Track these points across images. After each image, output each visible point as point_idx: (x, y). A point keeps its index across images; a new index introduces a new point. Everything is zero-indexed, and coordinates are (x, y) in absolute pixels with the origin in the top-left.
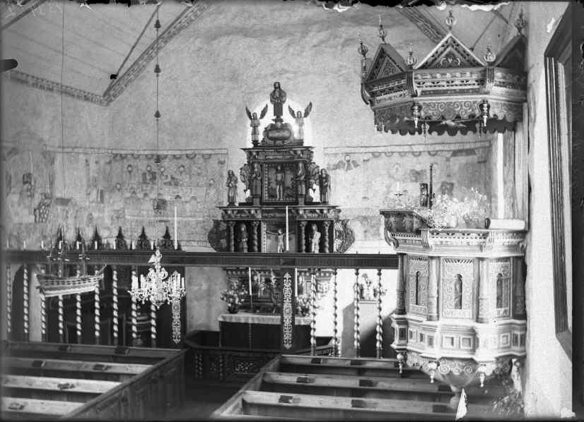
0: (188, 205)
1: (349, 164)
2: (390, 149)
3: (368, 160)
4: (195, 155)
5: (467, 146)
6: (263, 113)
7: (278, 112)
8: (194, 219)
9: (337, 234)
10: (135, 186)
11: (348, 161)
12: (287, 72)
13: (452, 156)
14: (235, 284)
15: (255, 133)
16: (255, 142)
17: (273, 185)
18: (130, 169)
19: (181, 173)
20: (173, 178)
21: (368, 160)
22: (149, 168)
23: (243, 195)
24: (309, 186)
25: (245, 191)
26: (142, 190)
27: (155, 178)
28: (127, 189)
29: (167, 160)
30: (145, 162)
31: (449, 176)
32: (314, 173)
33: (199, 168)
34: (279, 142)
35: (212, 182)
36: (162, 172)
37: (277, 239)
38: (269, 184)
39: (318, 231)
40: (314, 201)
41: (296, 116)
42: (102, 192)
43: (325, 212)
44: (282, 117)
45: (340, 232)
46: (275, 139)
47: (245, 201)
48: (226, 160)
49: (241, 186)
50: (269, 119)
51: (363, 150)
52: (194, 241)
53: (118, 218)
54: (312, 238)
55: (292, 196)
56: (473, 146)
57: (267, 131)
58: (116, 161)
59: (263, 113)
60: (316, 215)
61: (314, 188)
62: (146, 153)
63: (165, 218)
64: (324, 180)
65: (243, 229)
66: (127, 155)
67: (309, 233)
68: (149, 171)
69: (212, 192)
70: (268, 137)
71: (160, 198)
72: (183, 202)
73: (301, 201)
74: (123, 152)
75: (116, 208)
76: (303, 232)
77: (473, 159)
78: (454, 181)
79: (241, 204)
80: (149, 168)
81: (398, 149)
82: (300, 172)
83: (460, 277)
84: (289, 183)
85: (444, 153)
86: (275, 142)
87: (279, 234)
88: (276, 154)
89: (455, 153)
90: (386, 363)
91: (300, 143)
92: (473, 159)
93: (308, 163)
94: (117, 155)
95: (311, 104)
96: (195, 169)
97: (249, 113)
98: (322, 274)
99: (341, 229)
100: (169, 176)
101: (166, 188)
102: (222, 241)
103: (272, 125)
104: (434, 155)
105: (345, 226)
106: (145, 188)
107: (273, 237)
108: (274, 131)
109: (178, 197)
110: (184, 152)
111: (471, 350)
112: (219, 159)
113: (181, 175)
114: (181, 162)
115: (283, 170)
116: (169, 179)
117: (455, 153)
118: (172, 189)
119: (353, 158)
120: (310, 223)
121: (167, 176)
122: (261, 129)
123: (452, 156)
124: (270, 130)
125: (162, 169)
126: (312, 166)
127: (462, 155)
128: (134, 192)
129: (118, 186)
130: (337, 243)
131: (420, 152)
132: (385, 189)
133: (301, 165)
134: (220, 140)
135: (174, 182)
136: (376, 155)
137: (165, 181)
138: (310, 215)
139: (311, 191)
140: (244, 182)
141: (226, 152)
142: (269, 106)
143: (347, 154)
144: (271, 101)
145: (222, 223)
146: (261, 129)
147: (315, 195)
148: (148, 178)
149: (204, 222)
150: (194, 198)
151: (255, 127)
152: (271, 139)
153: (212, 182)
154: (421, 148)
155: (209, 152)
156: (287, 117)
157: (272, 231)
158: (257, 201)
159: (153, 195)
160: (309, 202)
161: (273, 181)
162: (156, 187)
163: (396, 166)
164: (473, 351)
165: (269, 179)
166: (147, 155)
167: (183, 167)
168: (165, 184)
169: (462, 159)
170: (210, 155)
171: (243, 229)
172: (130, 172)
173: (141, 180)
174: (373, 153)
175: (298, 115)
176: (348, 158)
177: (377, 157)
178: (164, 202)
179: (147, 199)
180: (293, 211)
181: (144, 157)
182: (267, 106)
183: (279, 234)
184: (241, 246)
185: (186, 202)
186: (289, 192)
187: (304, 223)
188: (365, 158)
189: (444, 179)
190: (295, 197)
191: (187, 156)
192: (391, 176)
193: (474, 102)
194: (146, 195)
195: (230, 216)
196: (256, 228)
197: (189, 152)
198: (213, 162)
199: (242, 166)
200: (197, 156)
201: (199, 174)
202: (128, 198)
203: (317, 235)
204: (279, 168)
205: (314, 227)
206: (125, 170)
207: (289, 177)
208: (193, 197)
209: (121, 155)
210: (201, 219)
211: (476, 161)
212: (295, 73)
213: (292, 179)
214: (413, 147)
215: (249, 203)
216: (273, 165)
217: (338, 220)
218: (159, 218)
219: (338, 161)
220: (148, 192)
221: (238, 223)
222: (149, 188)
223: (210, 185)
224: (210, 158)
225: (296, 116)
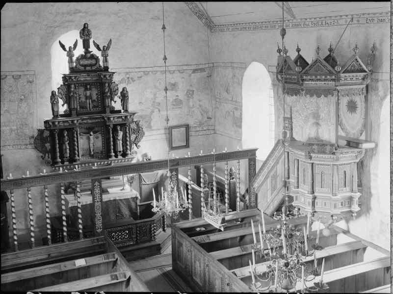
1: (130, 80)
2: (155, 69)
3: (141, 77)
4: (6, 76)
5: (201, 67)
6: (75, 45)
7: (86, 45)
11: (128, 78)
12: (80, 12)
13: (192, 73)
15: (71, 61)
16: (72, 70)
21: (141, 77)
23: (62, 109)
24: (112, 99)
25: (63, 105)
31: (191, 86)
34: (88, 68)
35: (23, 97)
37: (89, 139)
38: (79, 99)
39: (121, 130)
40: (115, 109)
41: (102, 49)
43: (129, 117)
44: (90, 50)
46: (85, 66)
47: (64, 113)
48: (34, 80)
49: (61, 102)
50: (79, 51)
51: (136, 70)
54: (118, 136)
55: (97, 107)
56: (203, 66)
57: (78, 59)
59: (75, 45)
60: (121, 120)
61: (115, 100)
65: (65, 135)
67: (115, 131)
69: (24, 105)
70: (80, 65)
73: (108, 110)
76: (111, 132)
77: (205, 74)
78: (194, 89)
79: (62, 116)
81: (158, 69)
83: (345, 172)
84: (95, 97)
85: (188, 71)
86: (85, 68)
87: (91, 135)
88: (86, 77)
89: (195, 71)
90: (231, 216)
91: (106, 69)
92: (205, 74)
93: (110, 82)
95: (111, 40)
97: (63, 46)
98: (126, 160)
103: (82, 55)
104: (182, 73)
105: (138, 125)
107: (85, 137)
108: (84, 60)
111: (348, 207)
112: (27, 78)
115: (90, 89)
117: (195, 71)
119: (131, 75)
120: (115, 126)
122: (74, 59)
123: (192, 73)
124: (80, 59)
126: (113, 85)
127: (198, 73)
130: (133, 137)
131: (174, 71)
132: (152, 96)
133: (107, 85)
134: (28, 63)
136: (146, 73)
138: (116, 120)
139: (112, 102)
140: (61, 98)
141: (33, 73)
142: (78, 42)
143: (127, 73)
144: (81, 37)
145: (45, 131)
146: (74, 59)
147: (117, 105)
151: (70, 55)
152: (82, 65)
153: (23, 97)
154: (174, 68)
155: (19, 73)
156: (93, 49)
160: (113, 111)
163: (160, 81)
164: (350, 207)
165: (79, 95)
169: (198, 75)
170: (20, 76)
171: (65, 135)
174: (144, 72)
175: (103, 49)
176: (128, 76)
177: (148, 74)
180: (106, 118)
182: (77, 41)
183: (91, 135)
184: (64, 148)
186: (95, 104)
187: (112, 126)
188: (139, 76)
189: (188, 88)
190: (103, 106)
192: (155, 87)
193: (360, 88)
195: (56, 126)
196: (75, 133)
198: (23, 81)
199: (59, 86)
200: (8, 77)
201: (10, 92)
203: (121, 134)
204: (88, 87)
205: (119, 128)
207: (94, 93)
208: (6, 110)
211: (206, 76)
212: (86, 13)
213: (97, 94)
214: (169, 67)
215: (66, 115)
216: (86, 86)
217: (133, 121)
219: (122, 77)
221: (61, 131)
223: (21, 99)
224: (19, 78)
225: (102, 49)
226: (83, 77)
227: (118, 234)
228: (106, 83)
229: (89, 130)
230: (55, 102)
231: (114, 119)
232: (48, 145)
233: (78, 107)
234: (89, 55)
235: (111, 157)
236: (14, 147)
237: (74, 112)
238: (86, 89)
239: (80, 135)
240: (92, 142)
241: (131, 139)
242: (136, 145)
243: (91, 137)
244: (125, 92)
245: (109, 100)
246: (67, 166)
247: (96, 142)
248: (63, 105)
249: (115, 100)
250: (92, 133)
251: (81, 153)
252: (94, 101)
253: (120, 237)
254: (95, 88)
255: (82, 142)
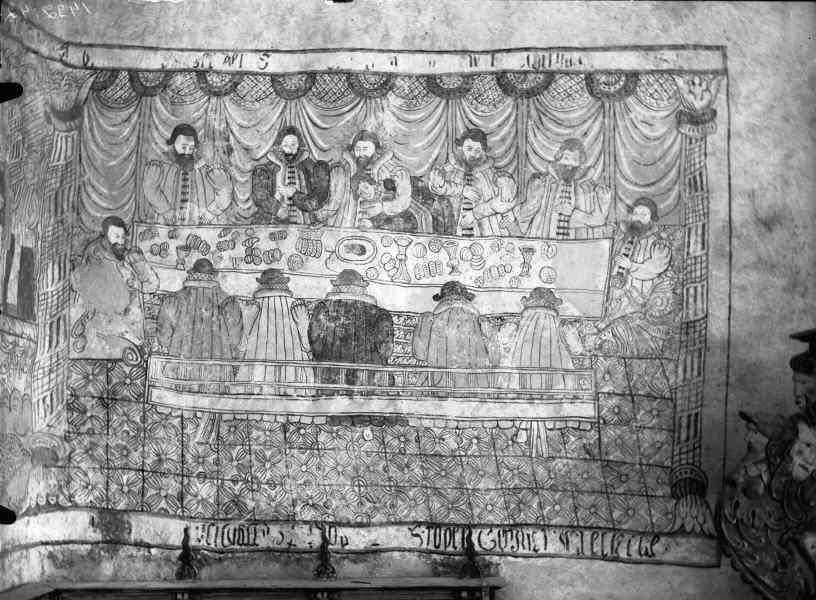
0: (505, 336)
4: (551, 76)
8: (542, 410)
10: (209, 235)
18: (183, 144)
19: (470, 166)
20: (422, 193)
22: (290, 143)
26: (251, 255)
27: (322, 195)
28: (162, 250)
29: (393, 100)
30: (272, 114)
33: (570, 144)
35: (643, 214)
36: (365, 164)
42: (27, 255)
52: (544, 528)
53: (107, 401)
58: (107, 105)
62: (275, 64)
63: (376, 406)
66: (169, 73)
68: (290, 159)
71: (347, 296)
72: (479, 320)
74: (154, 61)
75: (97, 348)
80: (290, 143)
94: (114, 72)
96: (545, 148)
100: (404, 186)
101: (386, 246)
106: (265, 244)
109: (450, 292)
110: (484, 64)
112: (677, 95)
113: (469, 179)
114: (469, 112)
116: (404, 200)
118: (417, 252)
121: (390, 186)
125: (366, 148)
128: (199, 266)
129: (115, 234)
135: (433, 216)
137: (377, 209)
148: (283, 190)
149: (599, 423)
150: (544, 298)
153: (643, 214)
155: (628, 61)
159: (312, 283)
162: (328, 240)
166: (275, 78)
167: (479, 135)
168: (382, 222)
170: (633, 76)
172: (184, 161)
173: (245, 206)
178: (376, 320)
179: (276, 301)
181: (265, 85)
185: (500, 320)
191: (501, 77)
194: (270, 280)
197: (513, 62)
200: (562, 82)
201: (569, 176)
202: (167, 297)
206: (158, 146)
209: (134, 74)
210: (587, 410)
218: (339, 405)
220: (282, 265)
222: (289, 246)
223: (635, 229)
236: (575, 540)
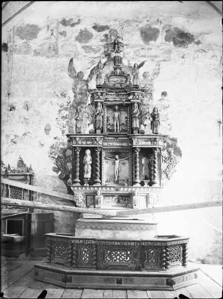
9: (164, 159)
14: (80, 199)
17: (111, 122)
32: (145, 113)
37: (114, 163)
38: (107, 122)
45: (166, 158)
55: (126, 131)
57: (108, 77)
64: (157, 116)
73: (136, 133)
82: (135, 110)
84: (123, 120)
88: (115, 96)
99: (167, 156)
102: (68, 164)
107: (110, 162)
115: (119, 110)
122: (103, 75)
130: (164, 166)
133: (136, 105)
145: (68, 150)
157: (111, 158)
158: (98, 132)
161: (111, 118)
183: (116, 159)
187: (139, 150)
204: (117, 108)
207: (124, 115)
213: (126, 118)
221: (83, 150)
226: (112, 98)
227: (116, 253)
228: (134, 103)
229: (115, 153)
230: (78, 118)
231: (139, 143)
232: (69, 166)
233: (106, 129)
234: (118, 71)
235: (134, 183)
237: (98, 132)
238: (115, 110)
239: (105, 159)
240: (117, 166)
241: (162, 168)
242: (167, 176)
243: (117, 162)
244: (156, 113)
245: (138, 122)
246: (86, 187)
247: (122, 168)
248: (89, 124)
249: (145, 124)
250: (117, 157)
251: (104, 178)
252: (123, 124)
253: (118, 257)
254: (125, 111)
255: (107, 167)
